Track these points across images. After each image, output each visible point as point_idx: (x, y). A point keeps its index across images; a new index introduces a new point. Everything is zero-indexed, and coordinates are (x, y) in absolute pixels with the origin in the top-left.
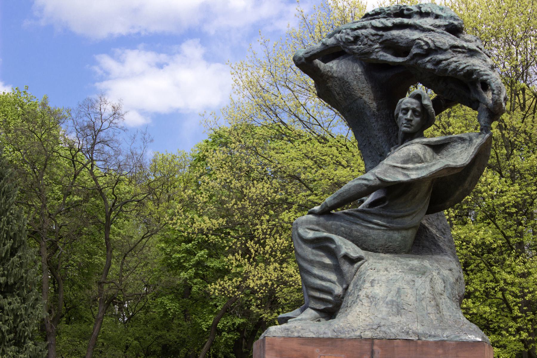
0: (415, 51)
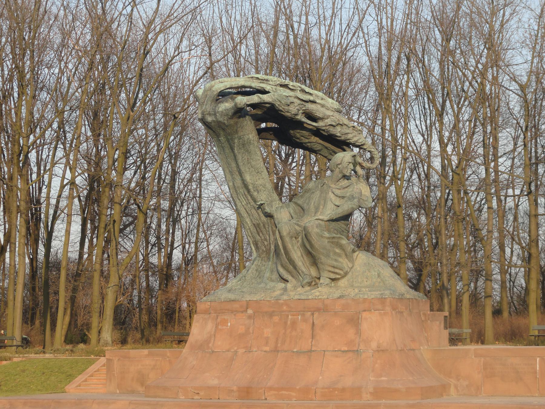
0: (328, 121)
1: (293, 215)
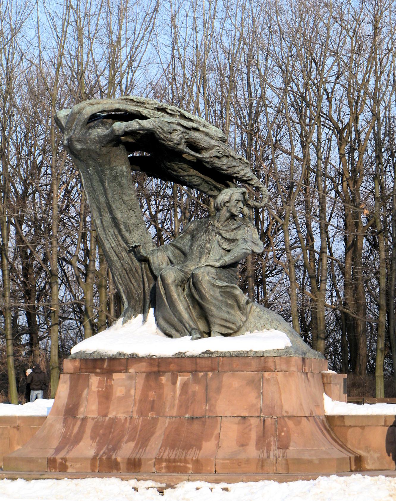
0: (213, 152)
1: (172, 259)
